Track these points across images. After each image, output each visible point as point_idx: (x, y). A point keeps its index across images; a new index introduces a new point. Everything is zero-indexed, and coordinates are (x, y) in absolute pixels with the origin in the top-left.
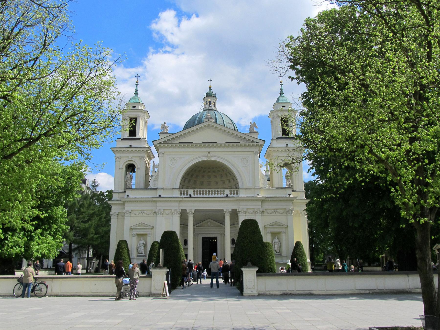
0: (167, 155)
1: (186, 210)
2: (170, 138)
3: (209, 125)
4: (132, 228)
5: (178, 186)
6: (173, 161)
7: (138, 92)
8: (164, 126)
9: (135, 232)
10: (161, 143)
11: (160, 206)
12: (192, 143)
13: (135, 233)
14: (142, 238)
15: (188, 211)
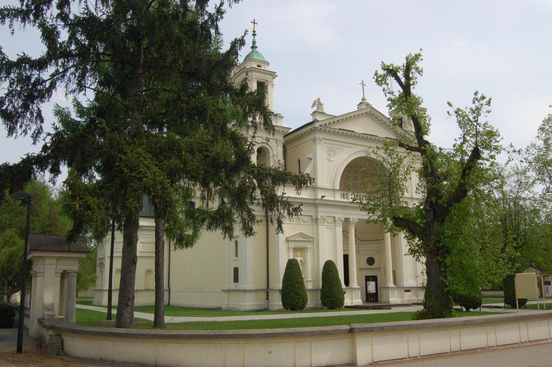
0: (325, 143)
1: (348, 218)
2: (331, 121)
3: (370, 112)
4: (291, 239)
5: (337, 187)
6: (331, 153)
7: (257, 45)
8: (318, 103)
9: (292, 245)
10: (321, 125)
11: (322, 212)
12: (353, 132)
13: (293, 246)
14: (299, 254)
15: (351, 220)
